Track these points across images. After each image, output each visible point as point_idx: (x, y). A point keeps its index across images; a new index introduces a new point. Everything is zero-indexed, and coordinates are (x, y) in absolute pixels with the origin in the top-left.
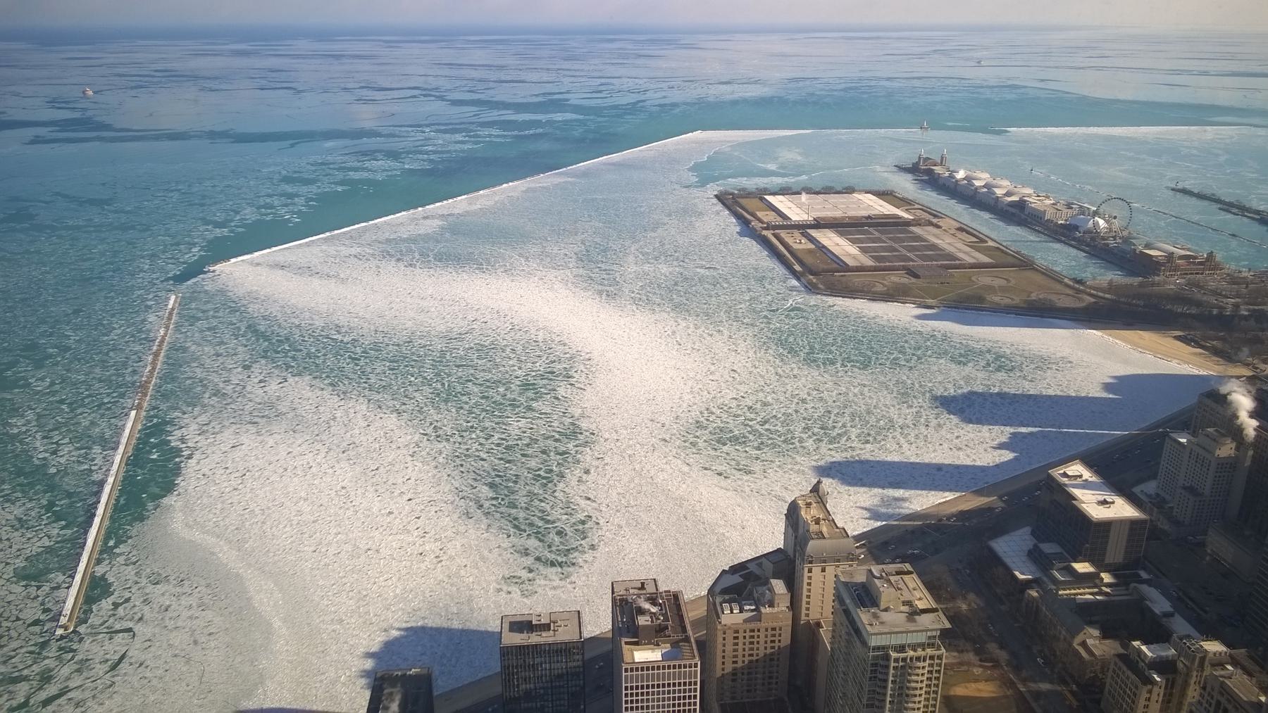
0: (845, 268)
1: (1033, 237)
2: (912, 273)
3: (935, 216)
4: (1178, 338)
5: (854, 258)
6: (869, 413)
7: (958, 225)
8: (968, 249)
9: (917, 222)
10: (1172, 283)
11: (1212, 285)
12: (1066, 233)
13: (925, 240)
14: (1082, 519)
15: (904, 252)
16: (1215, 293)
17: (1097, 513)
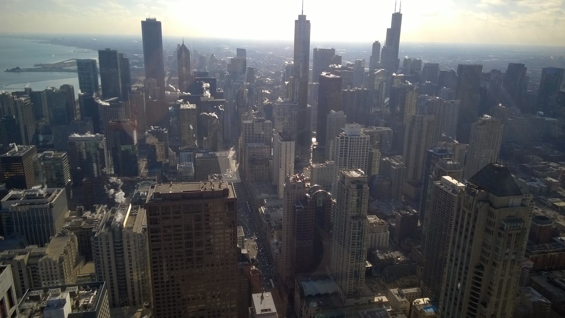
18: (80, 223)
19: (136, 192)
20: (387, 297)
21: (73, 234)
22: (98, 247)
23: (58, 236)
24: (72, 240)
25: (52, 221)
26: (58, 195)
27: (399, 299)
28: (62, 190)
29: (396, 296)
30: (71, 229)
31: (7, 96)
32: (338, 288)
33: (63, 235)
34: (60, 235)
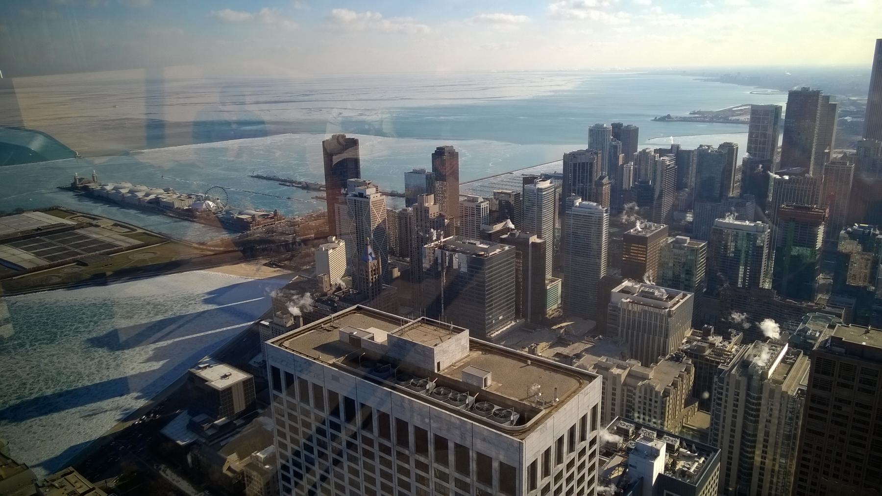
0: (23, 270)
1: (168, 220)
2: (81, 263)
3: (94, 219)
4: (265, 265)
5: (30, 261)
6: (59, 374)
7: (113, 223)
8: (124, 238)
9: (81, 226)
10: (257, 232)
11: (280, 230)
12: (189, 215)
13: (88, 238)
14: (214, 392)
15: (72, 249)
16: (283, 233)
17: (220, 385)
18: (703, 349)
19: (801, 326)
21: (690, 362)
22: (721, 394)
23: (669, 359)
24: (688, 370)
25: (667, 336)
26: (682, 301)
28: (689, 296)
30: (689, 353)
31: (648, 153)
33: (677, 359)
34: (672, 359)
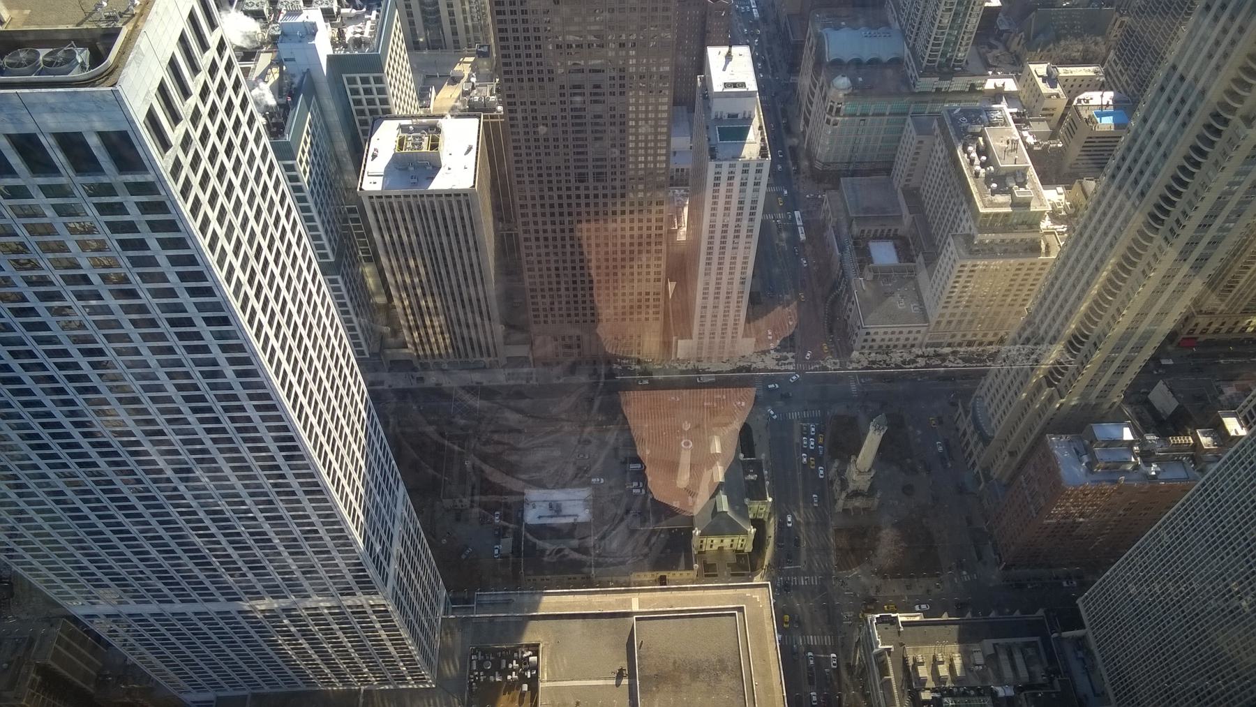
20: (1018, 79)
27: (1045, 88)
29: (1039, 81)
32: (907, 51)
